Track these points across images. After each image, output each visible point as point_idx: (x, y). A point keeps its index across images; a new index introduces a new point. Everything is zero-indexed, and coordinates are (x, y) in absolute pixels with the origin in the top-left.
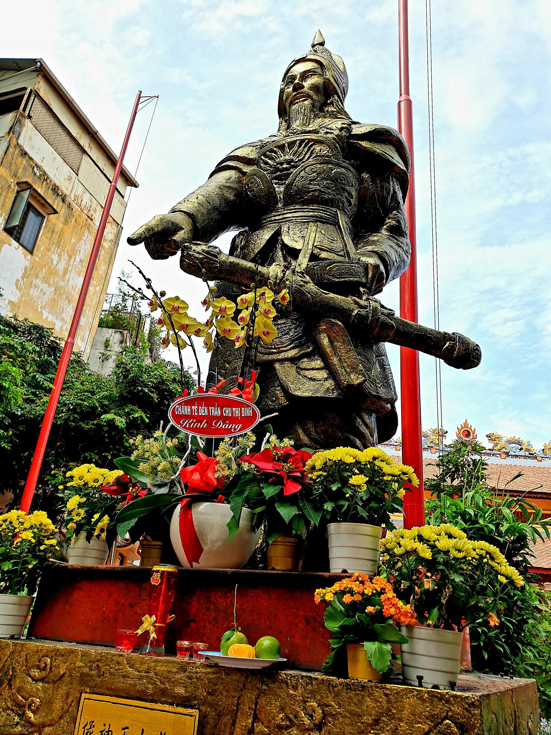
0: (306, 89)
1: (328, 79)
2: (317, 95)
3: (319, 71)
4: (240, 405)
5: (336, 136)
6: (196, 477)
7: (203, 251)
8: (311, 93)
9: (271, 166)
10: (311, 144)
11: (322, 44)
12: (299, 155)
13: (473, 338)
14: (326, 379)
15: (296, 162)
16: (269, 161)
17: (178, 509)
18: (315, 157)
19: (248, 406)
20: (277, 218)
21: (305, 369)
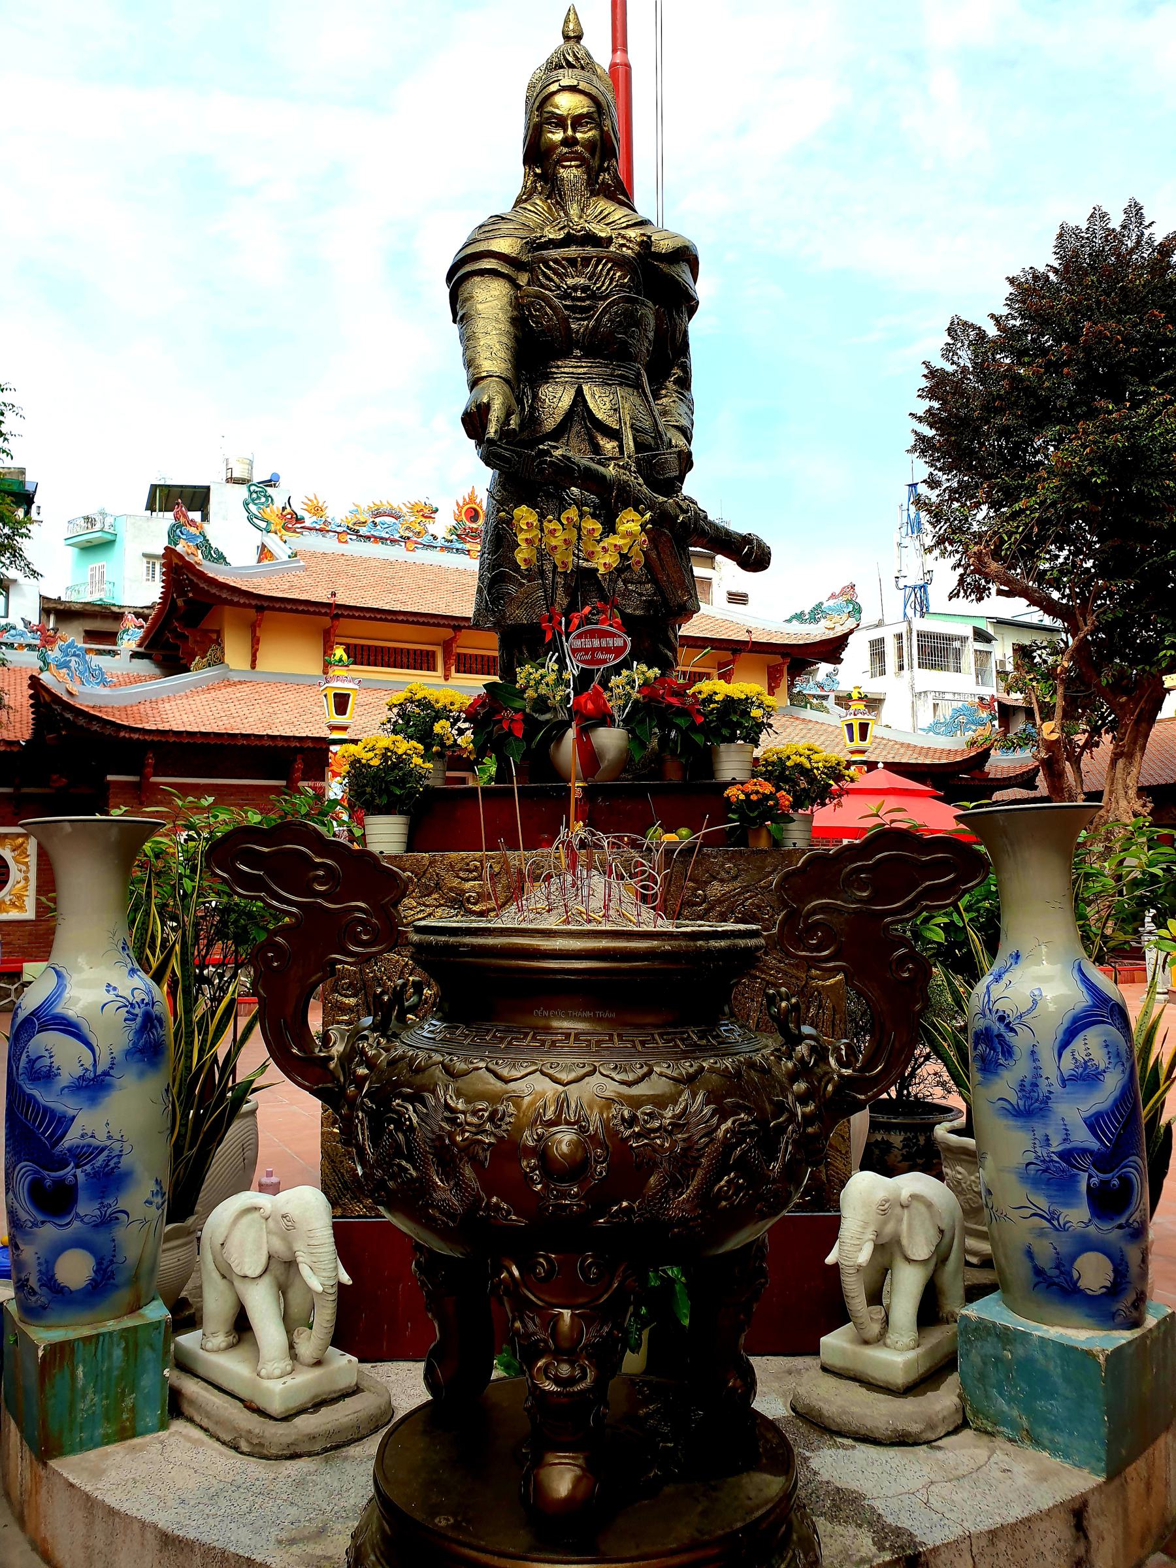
0: (579, 148)
1: (607, 133)
2: (593, 154)
3: (596, 116)
4: (613, 635)
5: (636, 254)
6: (590, 706)
7: (562, 455)
8: (587, 155)
9: (559, 287)
10: (610, 265)
11: (579, 38)
12: (597, 280)
13: (767, 540)
14: (654, 594)
15: (593, 292)
16: (555, 278)
17: (571, 734)
18: (615, 287)
19: (620, 636)
20: (574, 370)
21: (632, 583)
